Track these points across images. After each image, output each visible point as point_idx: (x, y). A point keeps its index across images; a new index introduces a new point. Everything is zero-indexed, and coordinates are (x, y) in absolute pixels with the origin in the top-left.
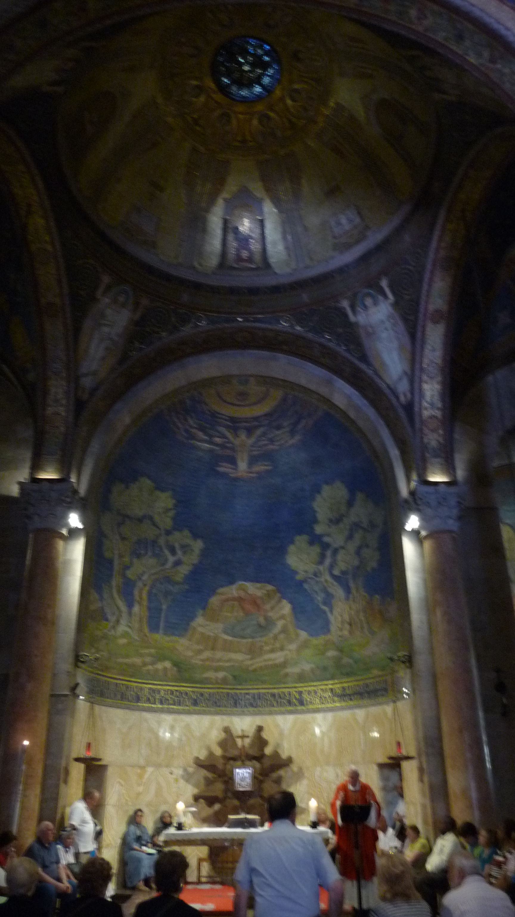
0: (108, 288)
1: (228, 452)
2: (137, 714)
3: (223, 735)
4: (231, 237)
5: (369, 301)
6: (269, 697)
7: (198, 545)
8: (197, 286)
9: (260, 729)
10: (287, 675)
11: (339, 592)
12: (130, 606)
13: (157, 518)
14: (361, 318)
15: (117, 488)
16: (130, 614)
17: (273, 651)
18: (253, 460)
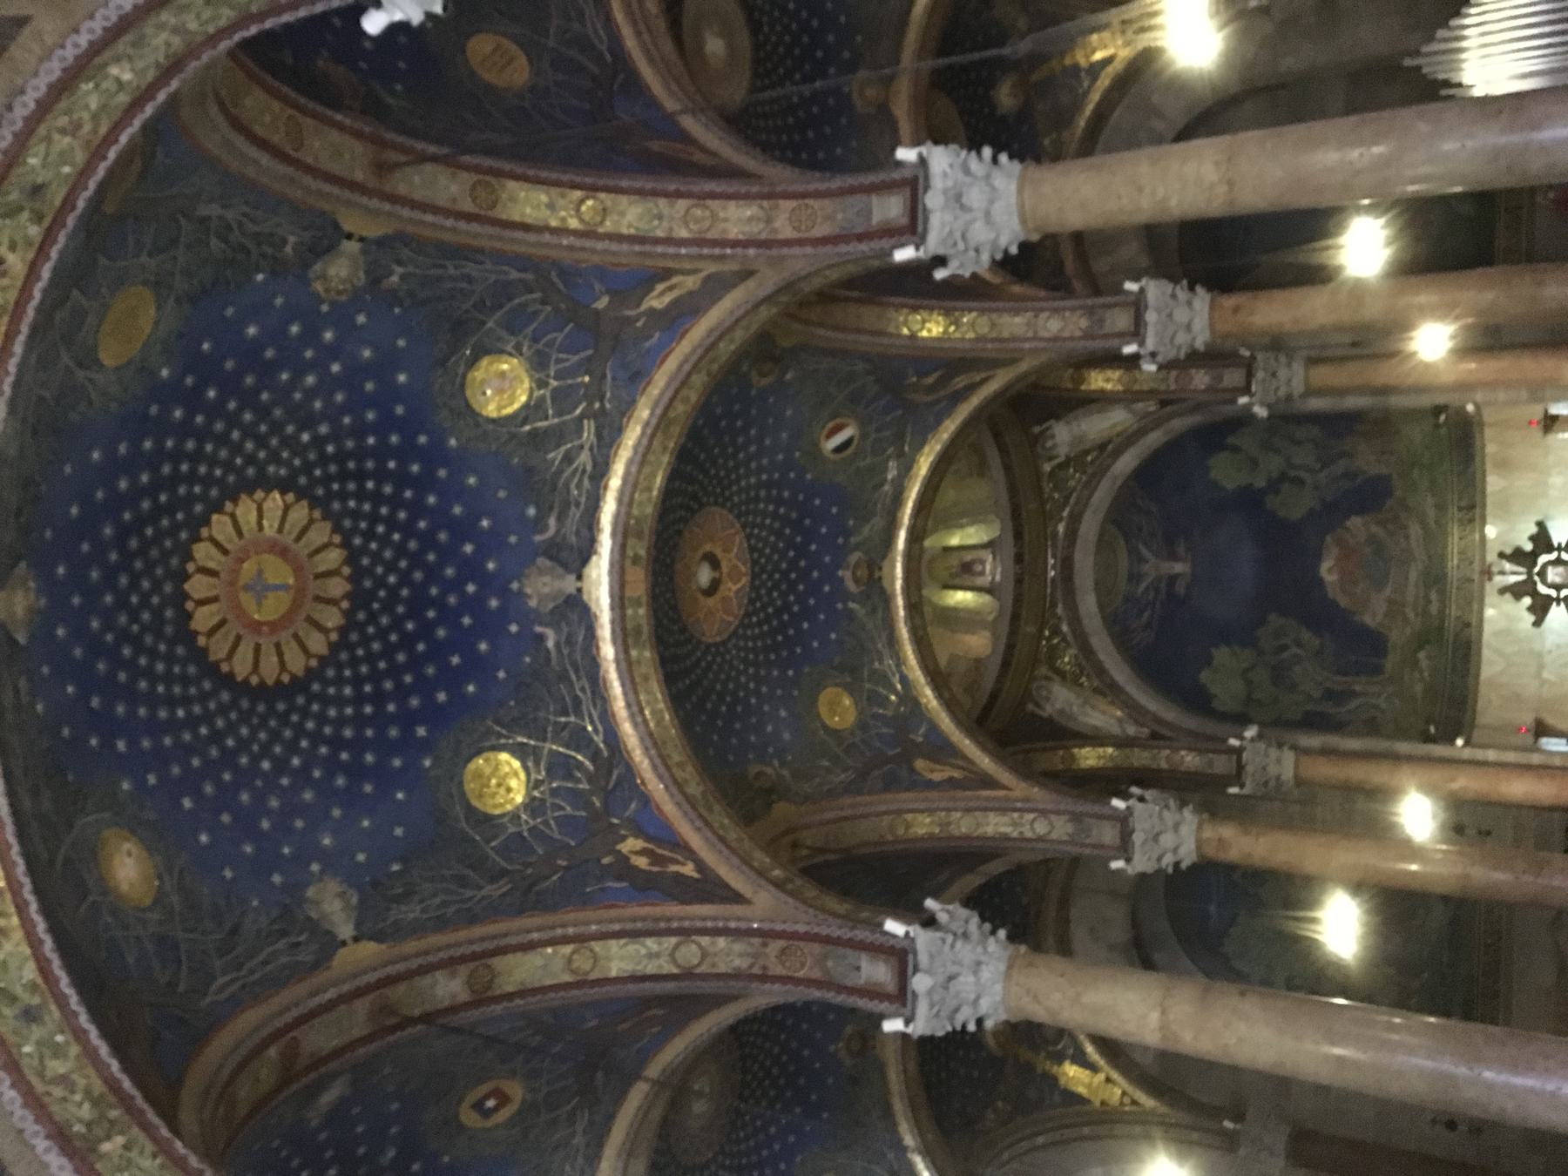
0: (1037, 705)
1: (1163, 585)
2: (1483, 689)
3: (1508, 596)
4: (957, 581)
5: (1049, 444)
6: (1463, 543)
7: (1274, 619)
8: (1015, 617)
9: (1502, 555)
10: (1436, 522)
11: (1341, 466)
12: (1354, 694)
13: (1245, 665)
14: (1063, 451)
15: (1216, 704)
16: (1364, 694)
17: (1407, 537)
18: (1173, 556)
